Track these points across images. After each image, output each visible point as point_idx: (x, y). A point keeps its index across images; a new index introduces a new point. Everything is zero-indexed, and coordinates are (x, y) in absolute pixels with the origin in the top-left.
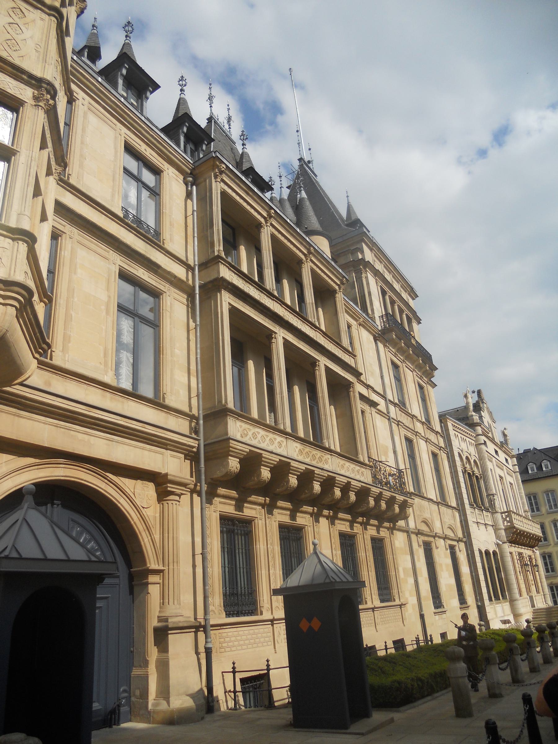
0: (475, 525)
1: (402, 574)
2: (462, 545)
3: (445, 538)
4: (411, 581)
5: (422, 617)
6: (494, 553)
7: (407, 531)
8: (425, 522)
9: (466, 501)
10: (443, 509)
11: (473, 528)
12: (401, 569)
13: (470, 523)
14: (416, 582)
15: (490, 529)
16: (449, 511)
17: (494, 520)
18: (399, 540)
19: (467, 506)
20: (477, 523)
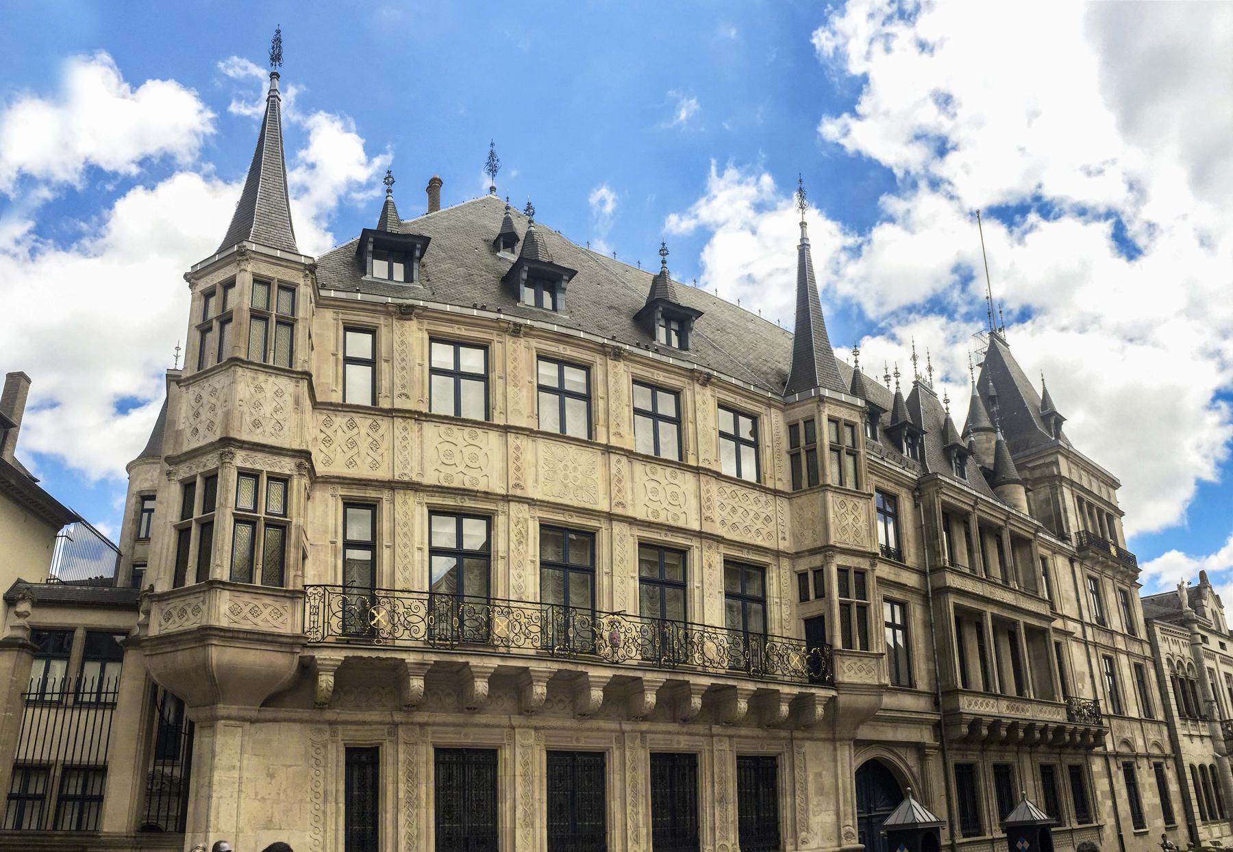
0: (1186, 739)
1: (1100, 798)
2: (1170, 763)
3: (1148, 756)
4: (1109, 803)
5: (1120, 837)
6: (1211, 766)
7: (1106, 757)
8: (1126, 742)
9: (1175, 713)
10: (1148, 726)
11: (1184, 743)
12: (1098, 793)
13: (1180, 737)
14: (1115, 803)
15: (1207, 741)
16: (1155, 727)
17: (1213, 730)
18: (1097, 766)
19: (1177, 719)
20: (1190, 736)
